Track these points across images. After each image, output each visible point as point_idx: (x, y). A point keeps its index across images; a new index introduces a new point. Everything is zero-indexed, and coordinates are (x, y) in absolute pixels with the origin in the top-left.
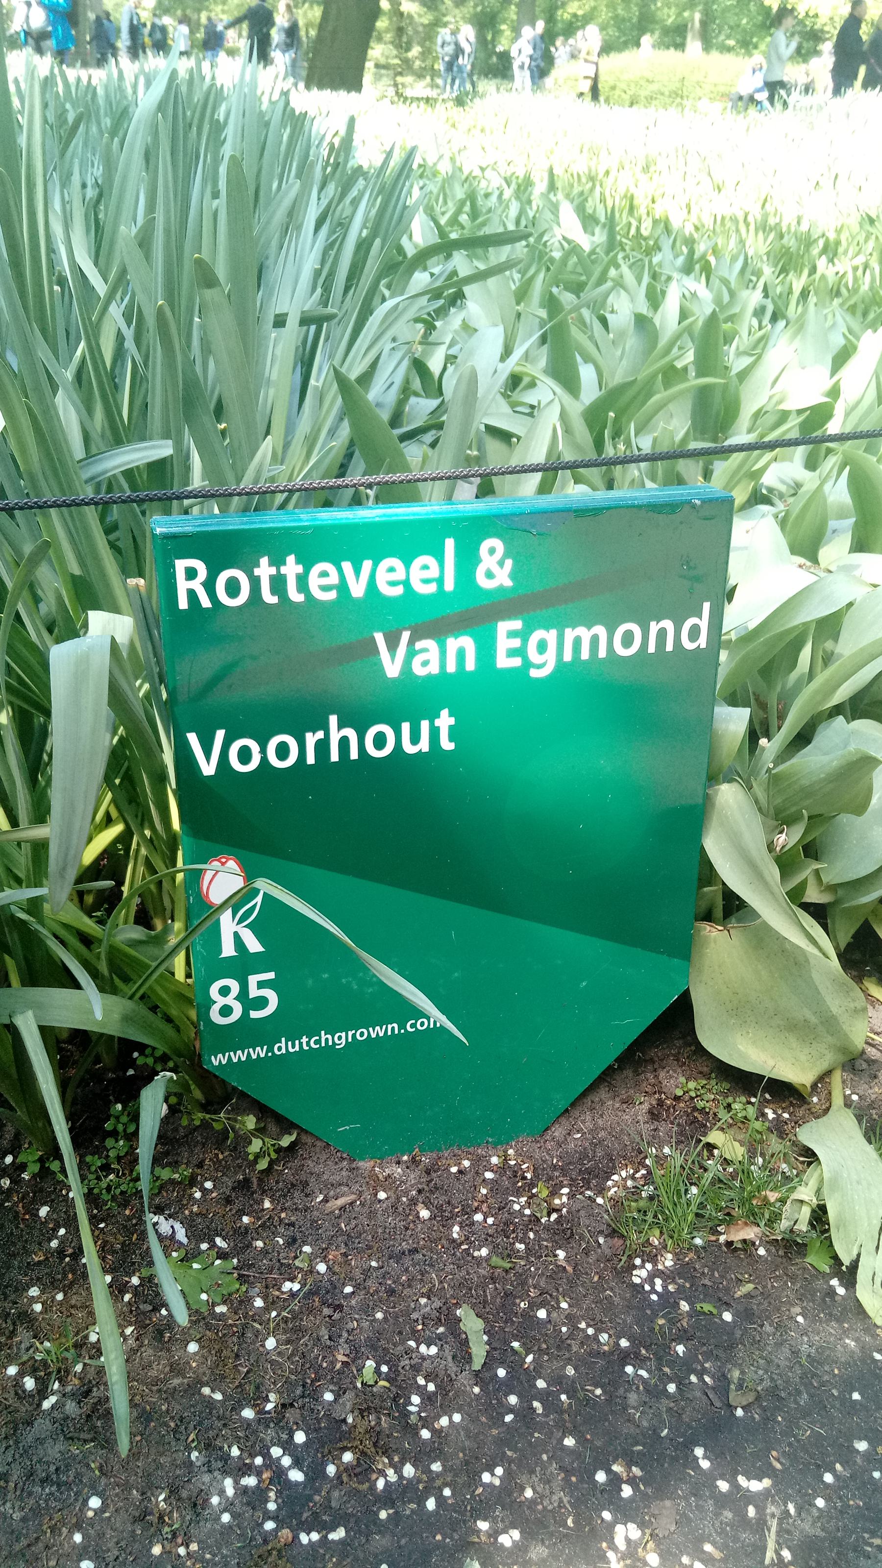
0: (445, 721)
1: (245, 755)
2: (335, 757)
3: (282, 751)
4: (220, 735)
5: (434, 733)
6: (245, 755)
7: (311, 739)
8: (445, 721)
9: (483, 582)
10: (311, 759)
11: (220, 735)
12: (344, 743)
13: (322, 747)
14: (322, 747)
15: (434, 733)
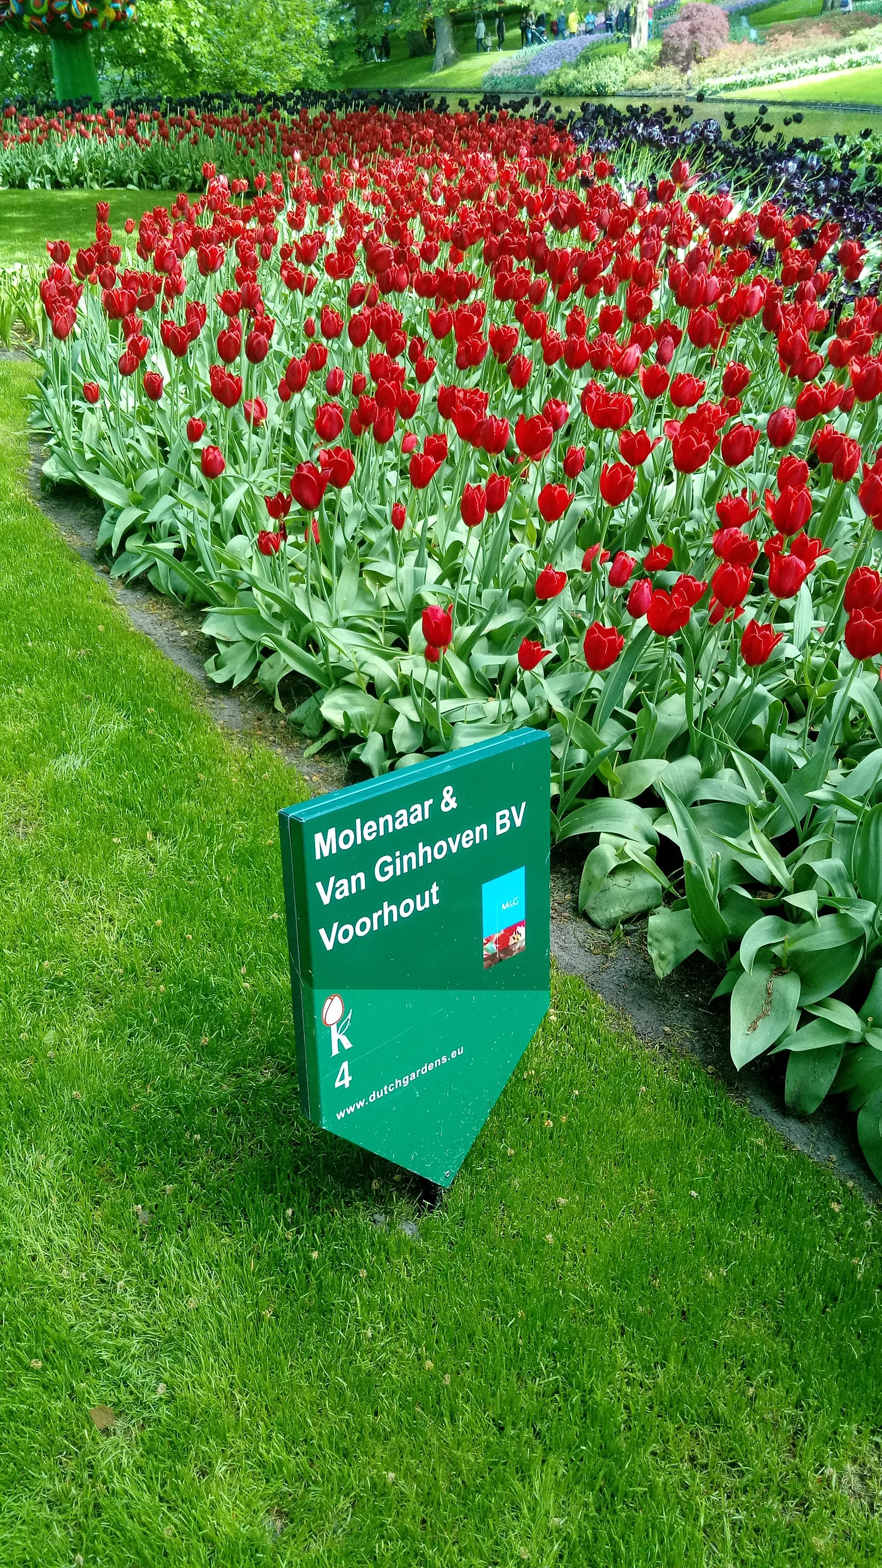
0: (435, 888)
1: (346, 934)
2: (386, 923)
3: (363, 926)
4: (336, 925)
5: (431, 895)
6: (346, 934)
7: (376, 916)
8: (435, 888)
9: (444, 809)
10: (375, 928)
11: (336, 925)
12: (391, 913)
13: (381, 919)
14: (381, 919)
15: (431, 895)
